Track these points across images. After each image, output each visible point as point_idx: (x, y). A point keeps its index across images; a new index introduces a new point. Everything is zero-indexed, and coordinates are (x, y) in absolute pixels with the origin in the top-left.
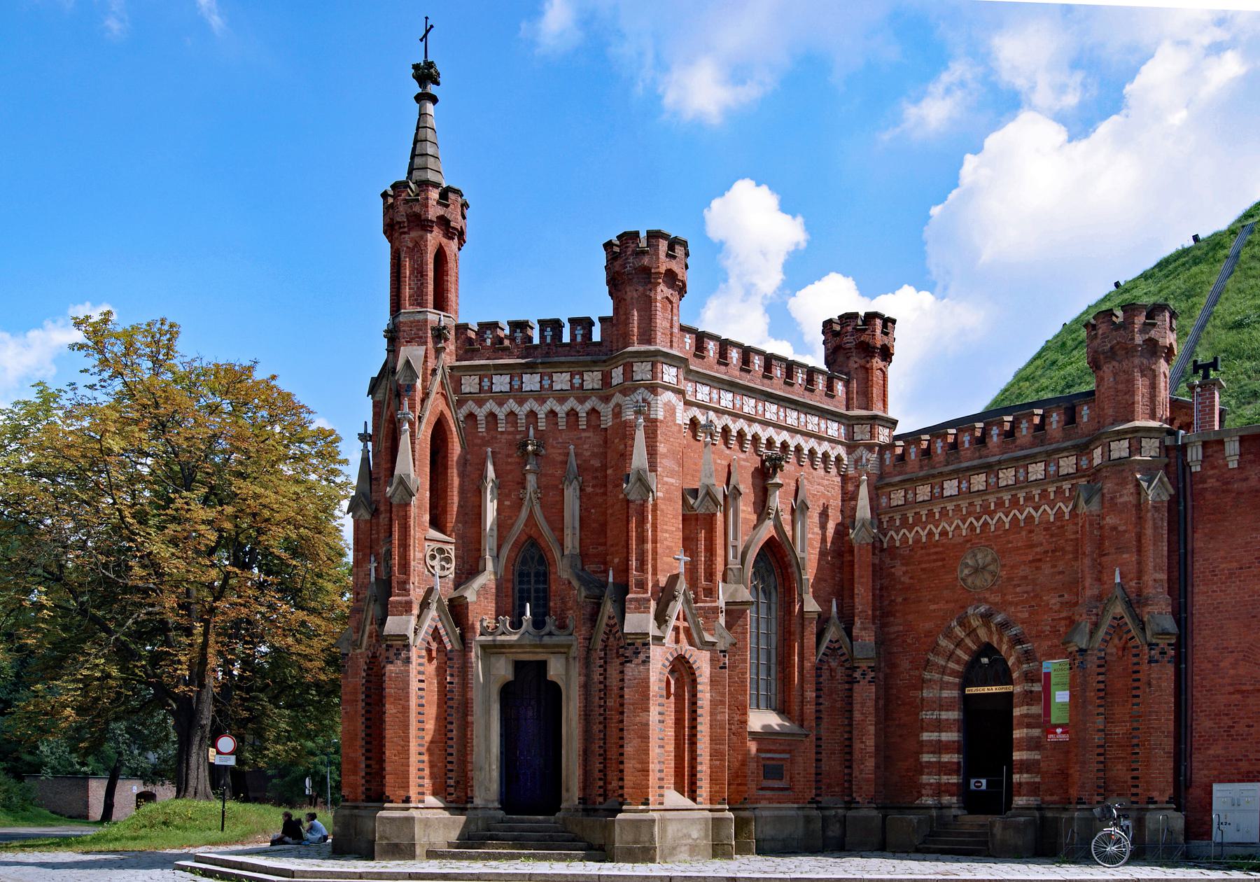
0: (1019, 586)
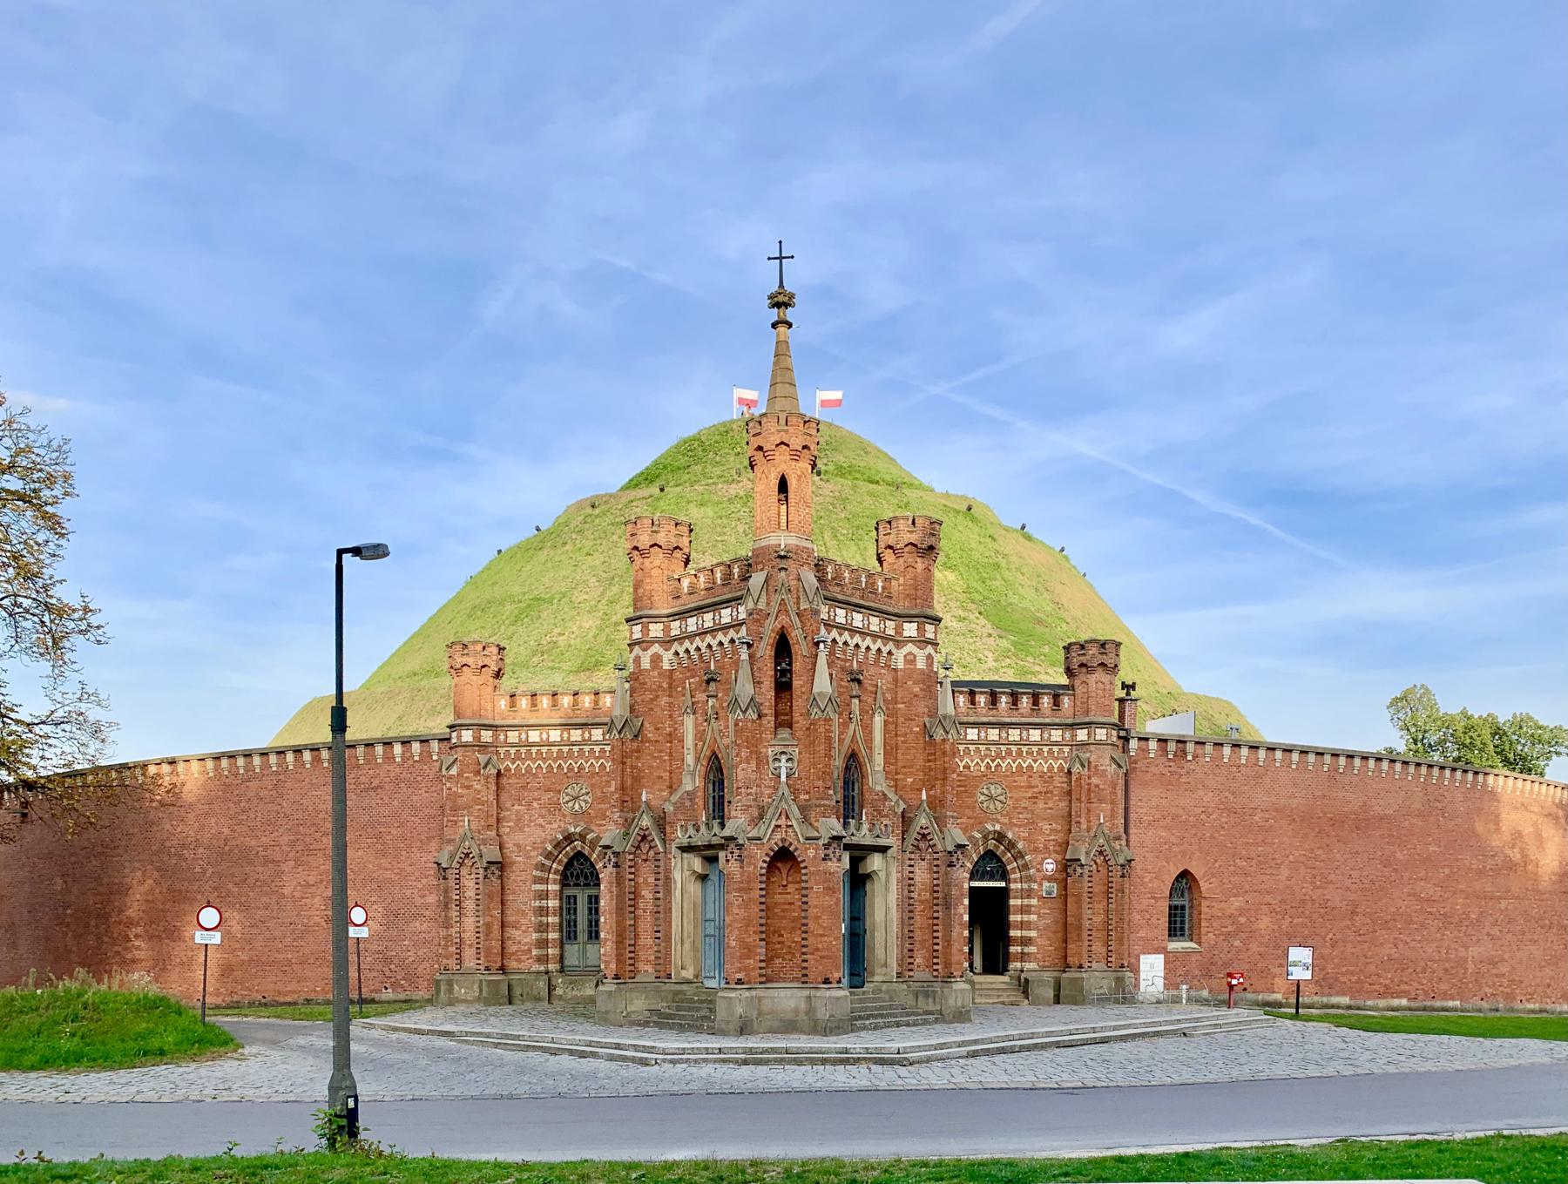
0: (1021, 813)
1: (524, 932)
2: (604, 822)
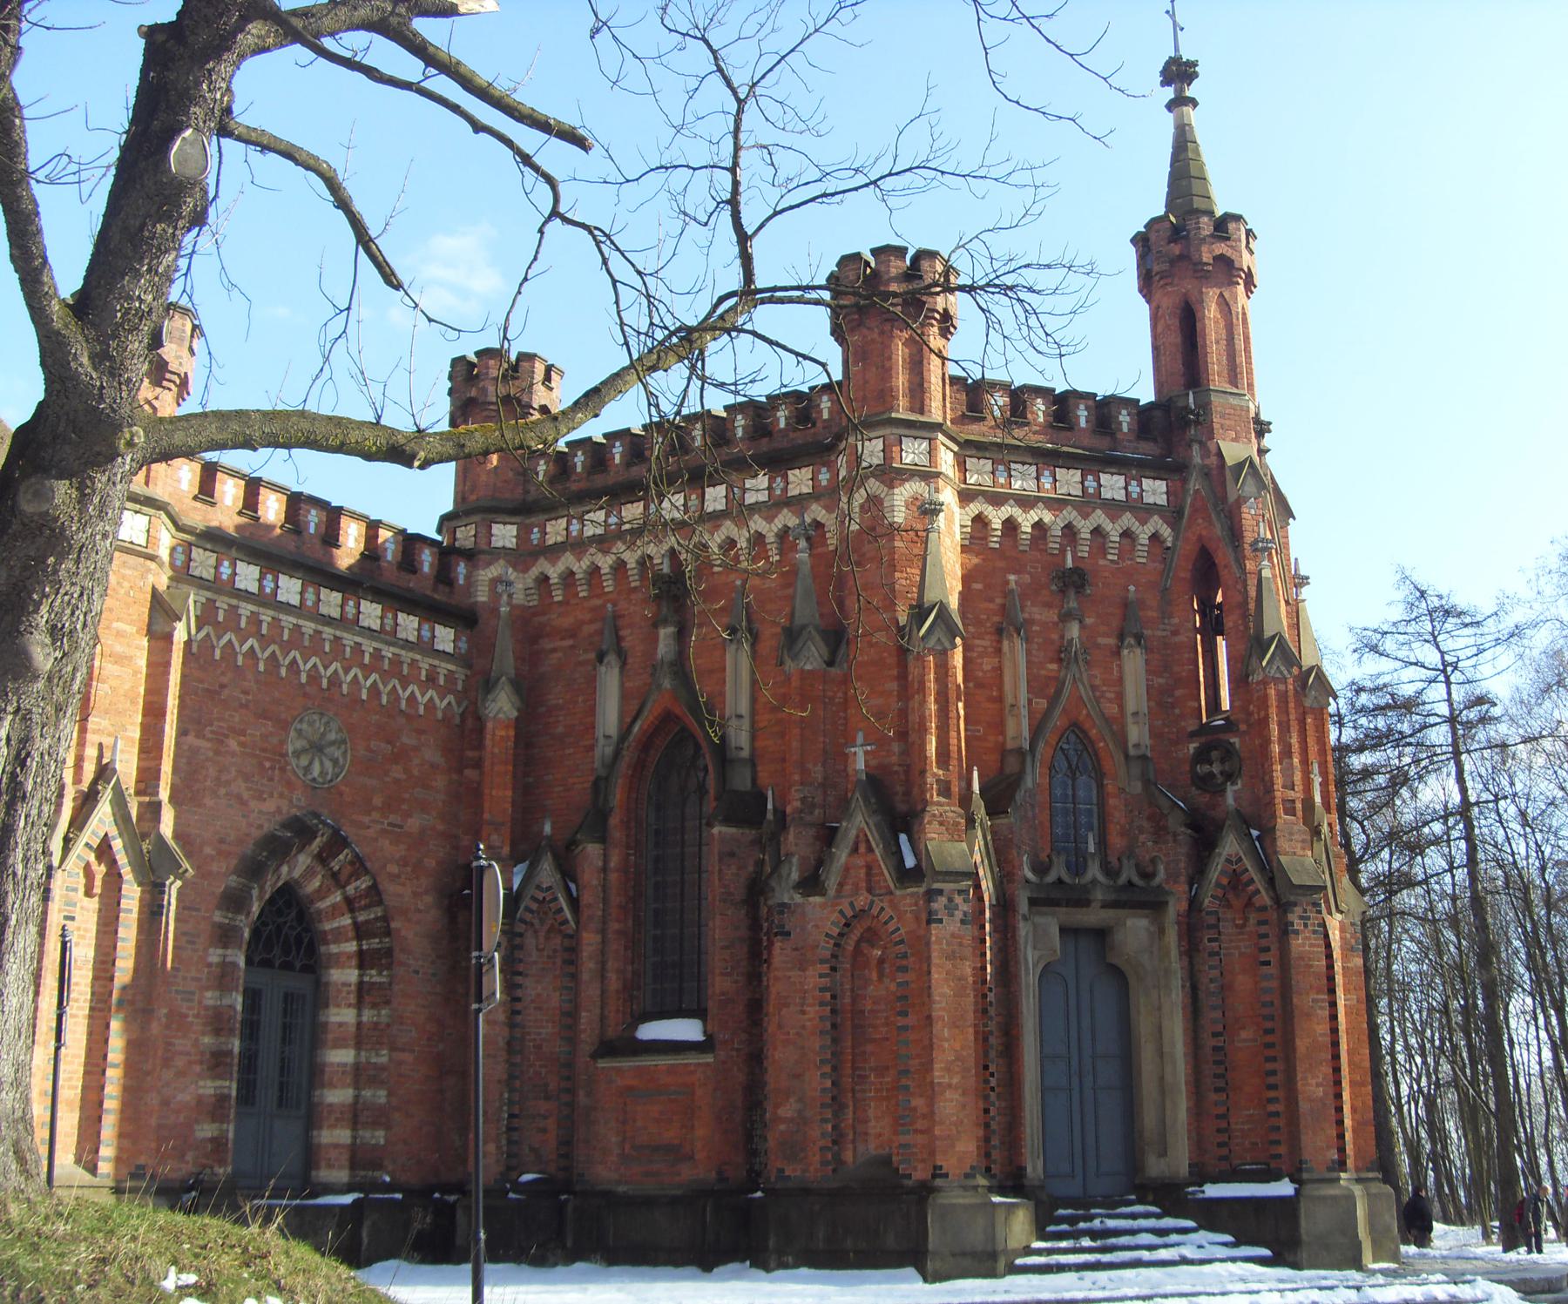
1: (181, 1074)
2: (366, 820)
